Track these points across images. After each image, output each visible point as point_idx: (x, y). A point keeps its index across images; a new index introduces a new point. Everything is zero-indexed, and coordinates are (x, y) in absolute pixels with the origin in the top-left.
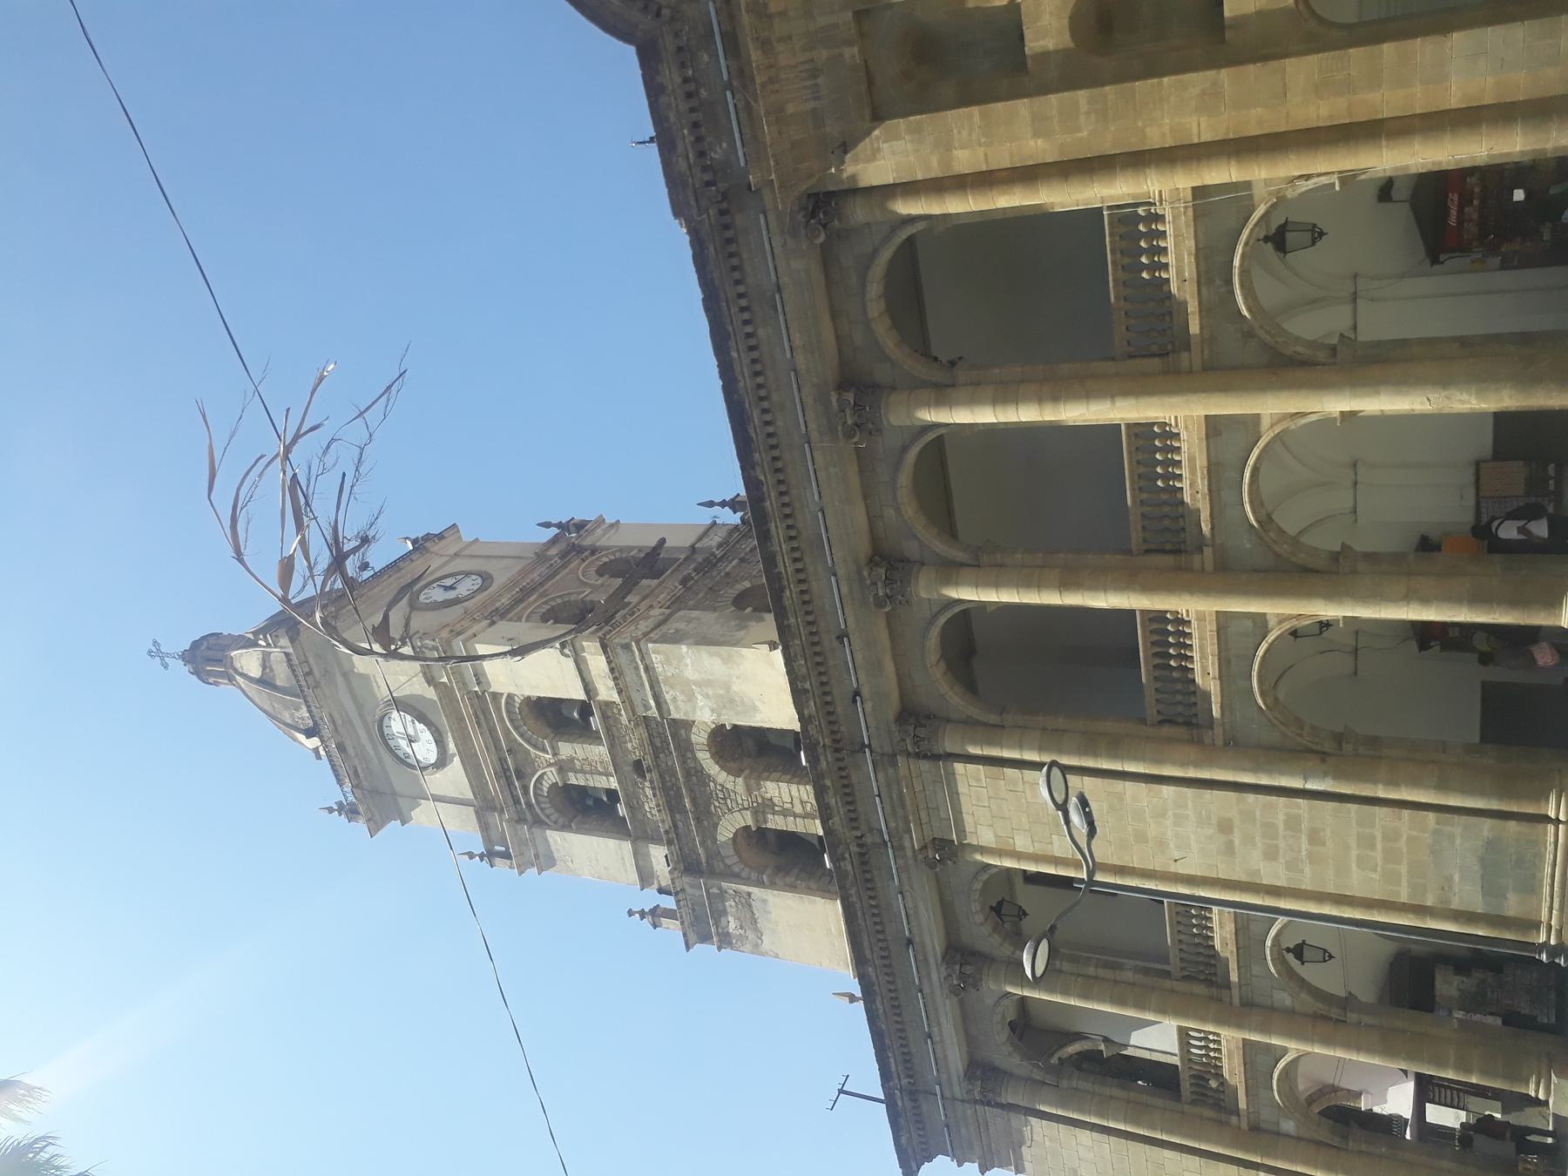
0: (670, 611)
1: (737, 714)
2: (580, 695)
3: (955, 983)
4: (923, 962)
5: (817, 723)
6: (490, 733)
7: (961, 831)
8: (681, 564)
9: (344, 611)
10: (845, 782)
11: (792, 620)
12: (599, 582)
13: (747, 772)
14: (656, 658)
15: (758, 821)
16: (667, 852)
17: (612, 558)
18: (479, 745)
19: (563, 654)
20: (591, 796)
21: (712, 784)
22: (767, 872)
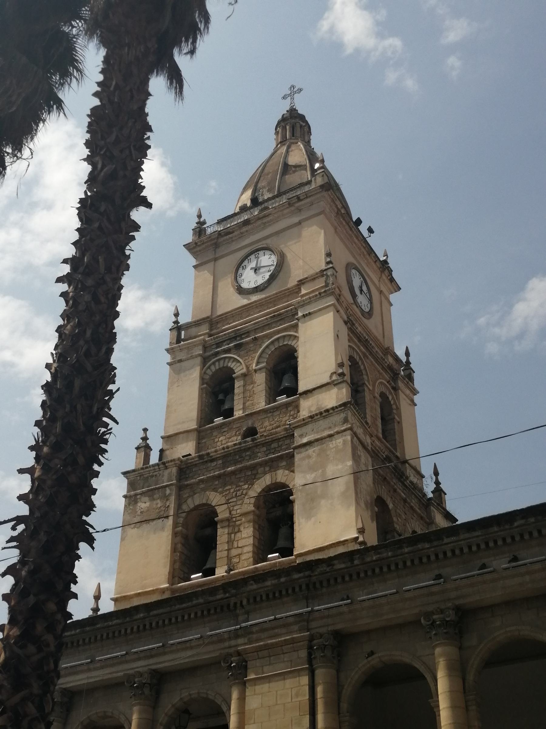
2: (302, 387)
3: (136, 680)
4: (150, 654)
7: (255, 681)
8: (393, 454)
10: (284, 593)
11: (406, 550)
12: (376, 395)
13: (257, 512)
14: (340, 443)
15: (222, 521)
16: (193, 455)
17: (392, 402)
20: (225, 397)
21: (246, 486)
22: (184, 530)
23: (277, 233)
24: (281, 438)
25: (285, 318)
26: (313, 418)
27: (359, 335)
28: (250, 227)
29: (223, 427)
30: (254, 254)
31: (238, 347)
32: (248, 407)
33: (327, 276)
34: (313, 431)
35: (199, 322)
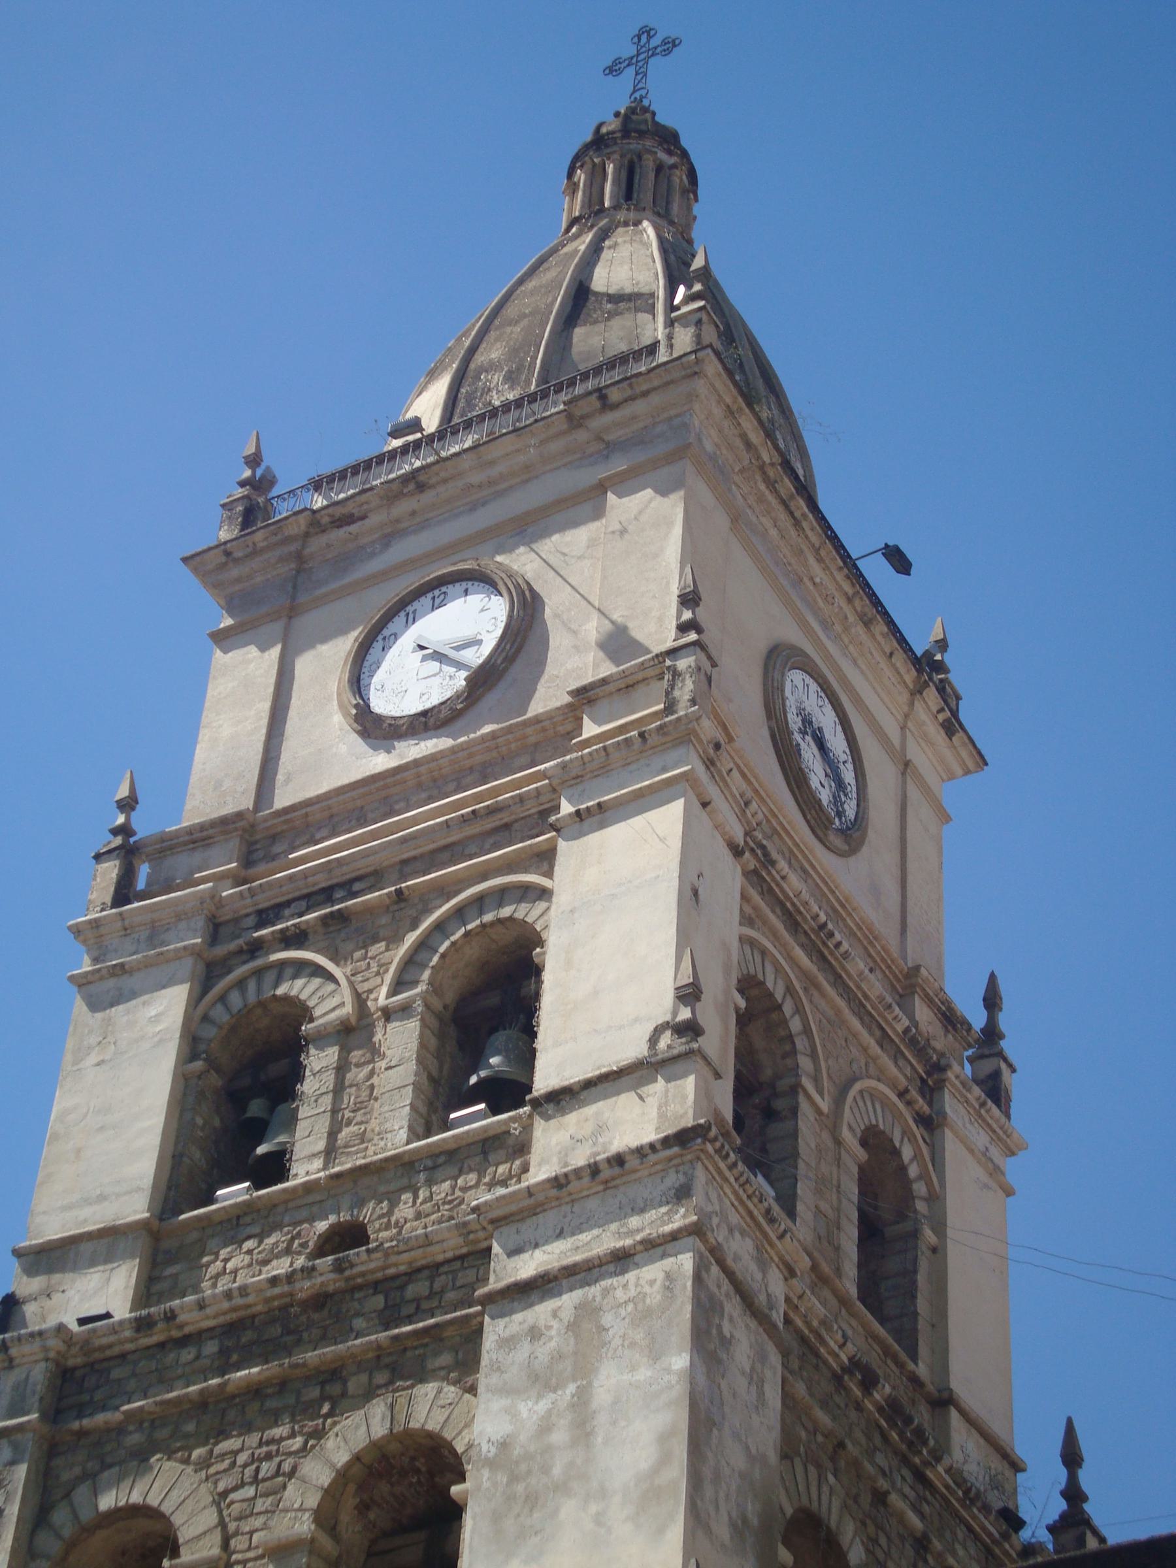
1: (497, 1518)
6: (446, 847)
8: (901, 1366)
9: (763, 487)
12: (846, 1134)
13: (327, 1543)
14: (652, 1283)
17: (913, 1171)
18: (415, 821)
19: (658, 1032)
20: (272, 1110)
21: (298, 1442)
24: (448, 1261)
27: (793, 904)
28: (428, 497)
29: (248, 1219)
30: (430, 595)
33: (676, 674)
35: (205, 834)
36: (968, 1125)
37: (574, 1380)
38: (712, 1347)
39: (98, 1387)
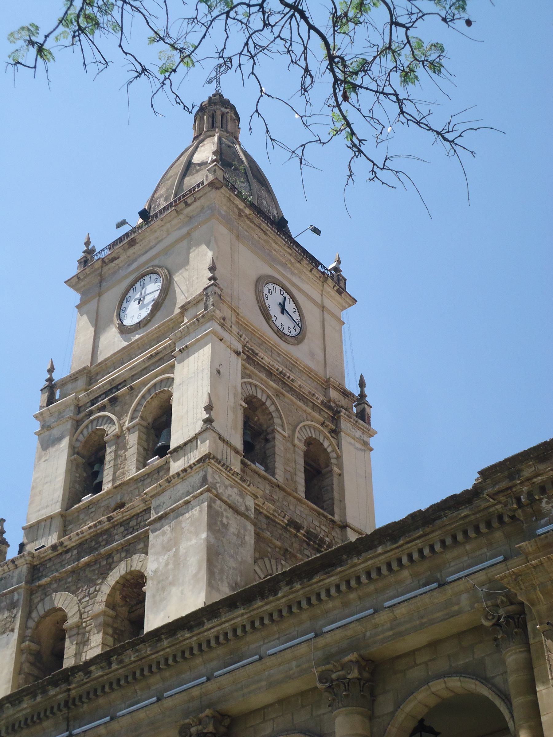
0: (252, 516)
1: (154, 596)
5: (85, 681)
6: (145, 369)
8: (325, 517)
9: (248, 222)
12: (296, 442)
13: (111, 612)
15: (71, 629)
17: (329, 450)
18: (137, 360)
22: (32, 644)
23: (166, 251)
24: (141, 512)
25: (163, 357)
26: (169, 482)
29: (91, 507)
30: (140, 281)
31: (113, 401)
32: (119, 476)
34: (170, 499)
35: (75, 377)
36: (351, 430)
37: (174, 547)
38: (217, 528)
39: (44, 570)
